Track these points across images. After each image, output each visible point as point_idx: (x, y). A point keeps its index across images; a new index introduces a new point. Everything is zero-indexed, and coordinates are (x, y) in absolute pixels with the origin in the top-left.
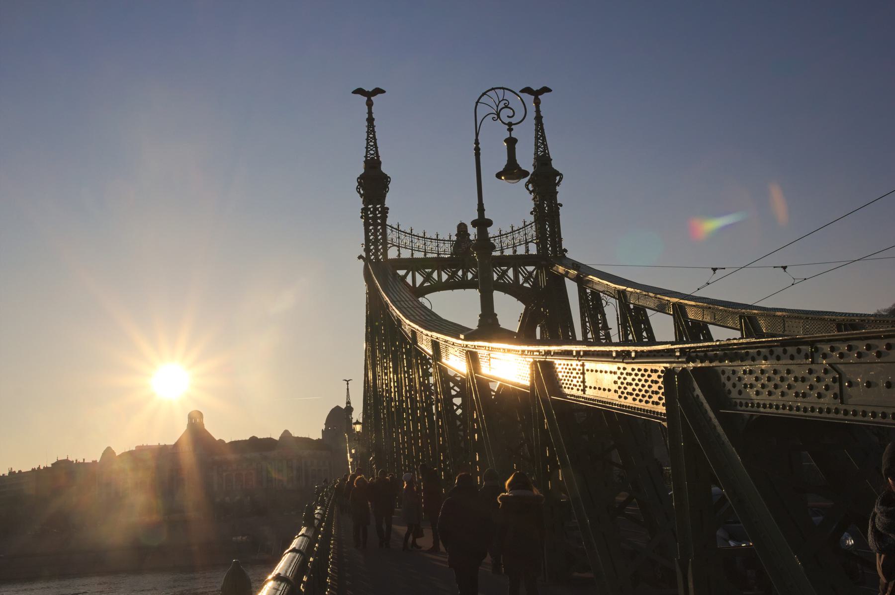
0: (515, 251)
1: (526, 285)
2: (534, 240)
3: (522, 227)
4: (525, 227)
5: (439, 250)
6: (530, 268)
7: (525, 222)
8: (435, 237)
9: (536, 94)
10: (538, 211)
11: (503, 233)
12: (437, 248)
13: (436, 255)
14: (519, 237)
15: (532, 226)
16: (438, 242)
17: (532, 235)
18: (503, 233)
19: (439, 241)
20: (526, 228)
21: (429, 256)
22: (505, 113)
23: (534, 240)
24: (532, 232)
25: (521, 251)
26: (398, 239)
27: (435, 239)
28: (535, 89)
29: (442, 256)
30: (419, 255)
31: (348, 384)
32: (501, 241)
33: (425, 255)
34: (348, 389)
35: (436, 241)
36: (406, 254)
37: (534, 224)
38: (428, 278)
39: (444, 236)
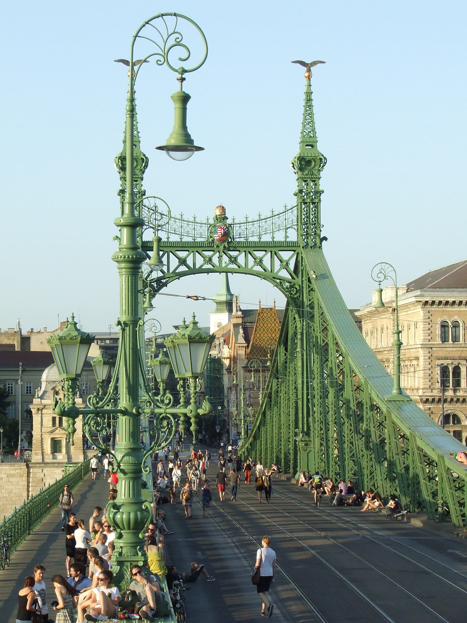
0: (273, 238)
1: (284, 274)
2: (295, 225)
3: (282, 212)
4: (285, 212)
5: (196, 233)
6: (285, 255)
8: (192, 220)
9: (308, 66)
11: (262, 217)
12: (193, 231)
13: (190, 239)
15: (292, 212)
16: (195, 225)
17: (292, 221)
19: (196, 224)
20: (287, 212)
21: (185, 239)
23: (295, 225)
24: (293, 216)
25: (280, 237)
26: (154, 221)
27: (192, 222)
29: (198, 240)
30: (174, 238)
32: (260, 226)
33: (181, 239)
35: (193, 224)
37: (296, 208)
38: (183, 262)
39: (201, 219)
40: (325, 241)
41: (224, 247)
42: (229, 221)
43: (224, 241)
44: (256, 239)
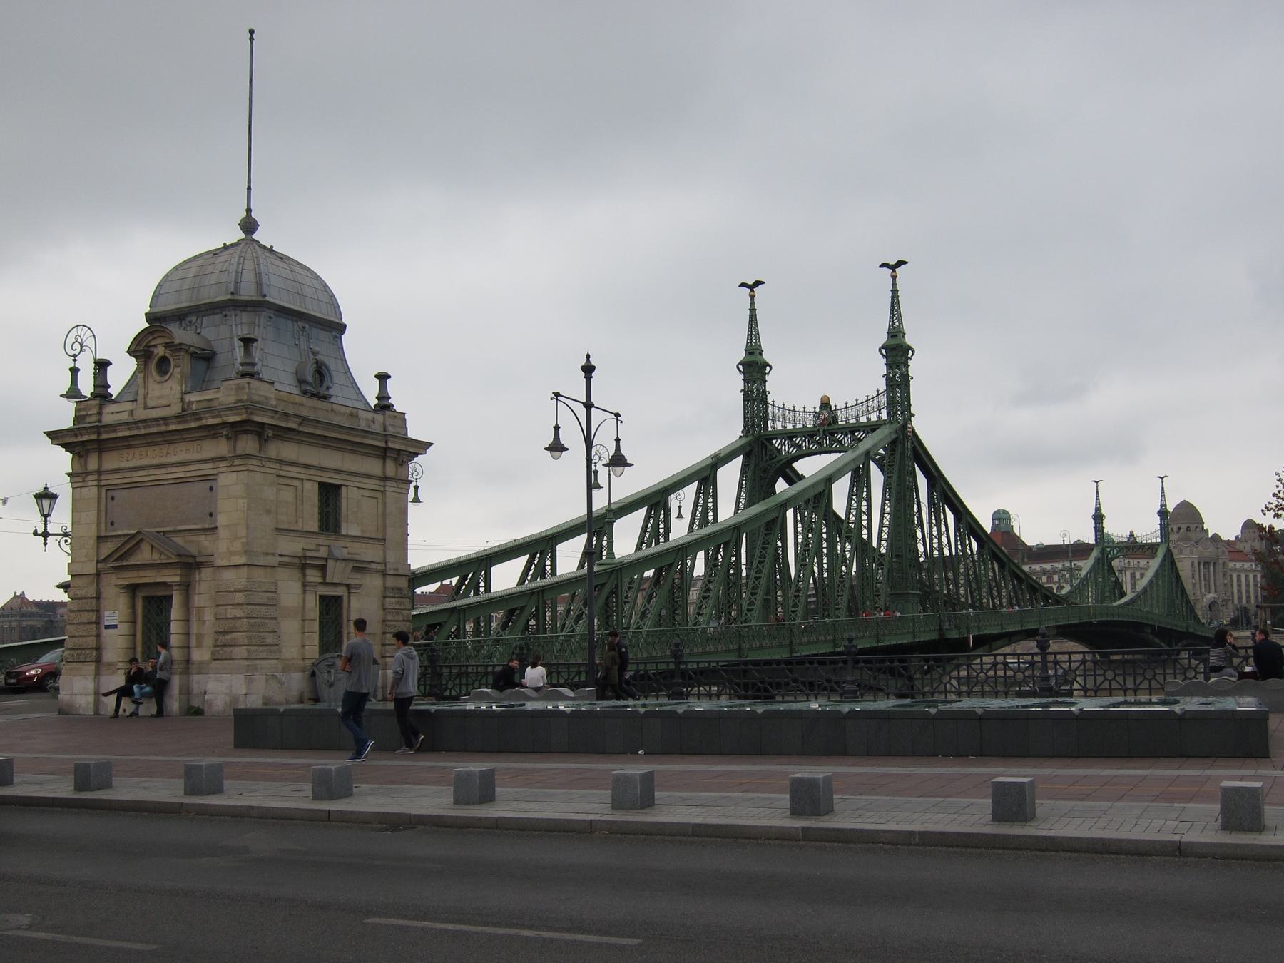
7: (878, 391)
9: (894, 268)
10: (890, 380)
11: (859, 402)
13: (801, 426)
14: (873, 404)
18: (859, 402)
21: (798, 426)
22: (416, 473)
25: (874, 417)
28: (891, 264)
29: (808, 426)
30: (790, 426)
31: (1097, 486)
34: (1097, 492)
36: (779, 426)
40: (912, 418)
41: (824, 430)
42: (833, 408)
43: (824, 425)
44: (854, 421)
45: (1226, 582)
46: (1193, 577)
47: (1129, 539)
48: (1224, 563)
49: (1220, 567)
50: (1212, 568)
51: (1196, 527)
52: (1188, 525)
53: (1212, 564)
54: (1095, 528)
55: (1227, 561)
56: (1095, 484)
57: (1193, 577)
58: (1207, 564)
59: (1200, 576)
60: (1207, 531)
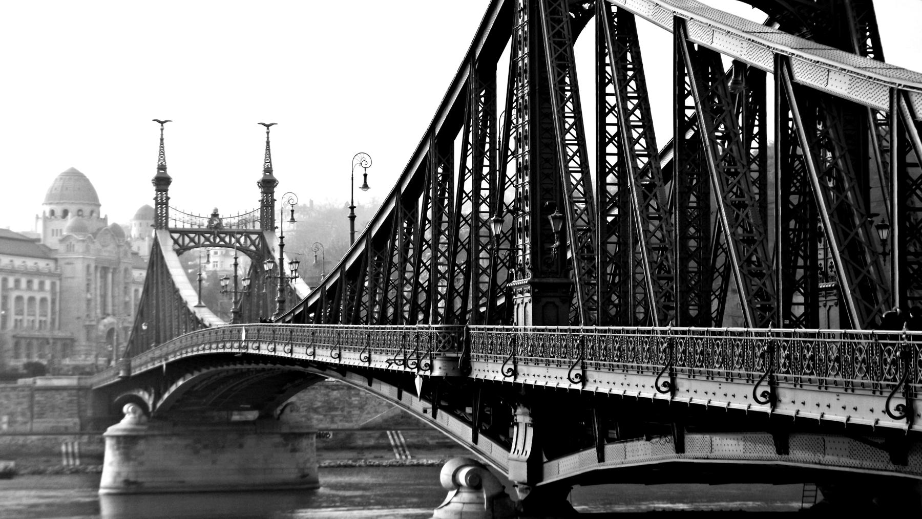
45: (127, 299)
46: (88, 290)
47: (211, 221)
48: (126, 270)
49: (120, 276)
50: (110, 276)
51: (92, 212)
52: (81, 207)
53: (111, 270)
54: (156, 199)
55: (130, 267)
56: (160, 124)
57: (88, 290)
58: (105, 270)
59: (96, 288)
60: (105, 220)
